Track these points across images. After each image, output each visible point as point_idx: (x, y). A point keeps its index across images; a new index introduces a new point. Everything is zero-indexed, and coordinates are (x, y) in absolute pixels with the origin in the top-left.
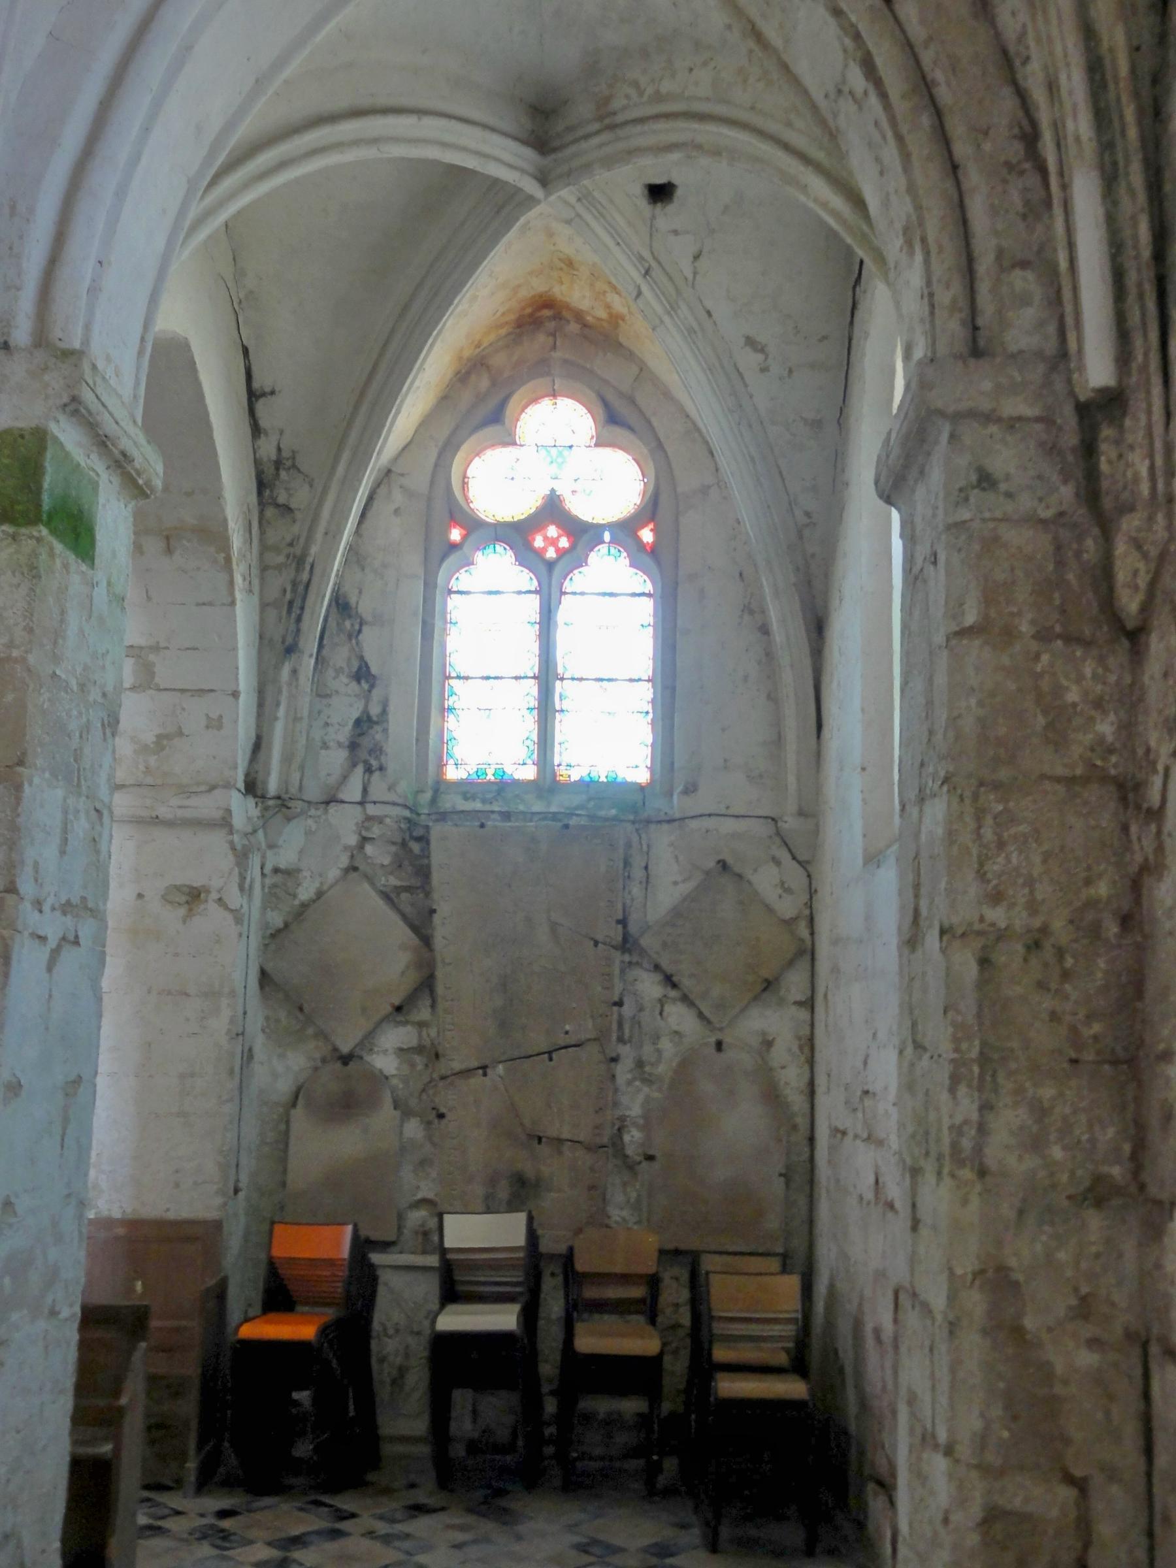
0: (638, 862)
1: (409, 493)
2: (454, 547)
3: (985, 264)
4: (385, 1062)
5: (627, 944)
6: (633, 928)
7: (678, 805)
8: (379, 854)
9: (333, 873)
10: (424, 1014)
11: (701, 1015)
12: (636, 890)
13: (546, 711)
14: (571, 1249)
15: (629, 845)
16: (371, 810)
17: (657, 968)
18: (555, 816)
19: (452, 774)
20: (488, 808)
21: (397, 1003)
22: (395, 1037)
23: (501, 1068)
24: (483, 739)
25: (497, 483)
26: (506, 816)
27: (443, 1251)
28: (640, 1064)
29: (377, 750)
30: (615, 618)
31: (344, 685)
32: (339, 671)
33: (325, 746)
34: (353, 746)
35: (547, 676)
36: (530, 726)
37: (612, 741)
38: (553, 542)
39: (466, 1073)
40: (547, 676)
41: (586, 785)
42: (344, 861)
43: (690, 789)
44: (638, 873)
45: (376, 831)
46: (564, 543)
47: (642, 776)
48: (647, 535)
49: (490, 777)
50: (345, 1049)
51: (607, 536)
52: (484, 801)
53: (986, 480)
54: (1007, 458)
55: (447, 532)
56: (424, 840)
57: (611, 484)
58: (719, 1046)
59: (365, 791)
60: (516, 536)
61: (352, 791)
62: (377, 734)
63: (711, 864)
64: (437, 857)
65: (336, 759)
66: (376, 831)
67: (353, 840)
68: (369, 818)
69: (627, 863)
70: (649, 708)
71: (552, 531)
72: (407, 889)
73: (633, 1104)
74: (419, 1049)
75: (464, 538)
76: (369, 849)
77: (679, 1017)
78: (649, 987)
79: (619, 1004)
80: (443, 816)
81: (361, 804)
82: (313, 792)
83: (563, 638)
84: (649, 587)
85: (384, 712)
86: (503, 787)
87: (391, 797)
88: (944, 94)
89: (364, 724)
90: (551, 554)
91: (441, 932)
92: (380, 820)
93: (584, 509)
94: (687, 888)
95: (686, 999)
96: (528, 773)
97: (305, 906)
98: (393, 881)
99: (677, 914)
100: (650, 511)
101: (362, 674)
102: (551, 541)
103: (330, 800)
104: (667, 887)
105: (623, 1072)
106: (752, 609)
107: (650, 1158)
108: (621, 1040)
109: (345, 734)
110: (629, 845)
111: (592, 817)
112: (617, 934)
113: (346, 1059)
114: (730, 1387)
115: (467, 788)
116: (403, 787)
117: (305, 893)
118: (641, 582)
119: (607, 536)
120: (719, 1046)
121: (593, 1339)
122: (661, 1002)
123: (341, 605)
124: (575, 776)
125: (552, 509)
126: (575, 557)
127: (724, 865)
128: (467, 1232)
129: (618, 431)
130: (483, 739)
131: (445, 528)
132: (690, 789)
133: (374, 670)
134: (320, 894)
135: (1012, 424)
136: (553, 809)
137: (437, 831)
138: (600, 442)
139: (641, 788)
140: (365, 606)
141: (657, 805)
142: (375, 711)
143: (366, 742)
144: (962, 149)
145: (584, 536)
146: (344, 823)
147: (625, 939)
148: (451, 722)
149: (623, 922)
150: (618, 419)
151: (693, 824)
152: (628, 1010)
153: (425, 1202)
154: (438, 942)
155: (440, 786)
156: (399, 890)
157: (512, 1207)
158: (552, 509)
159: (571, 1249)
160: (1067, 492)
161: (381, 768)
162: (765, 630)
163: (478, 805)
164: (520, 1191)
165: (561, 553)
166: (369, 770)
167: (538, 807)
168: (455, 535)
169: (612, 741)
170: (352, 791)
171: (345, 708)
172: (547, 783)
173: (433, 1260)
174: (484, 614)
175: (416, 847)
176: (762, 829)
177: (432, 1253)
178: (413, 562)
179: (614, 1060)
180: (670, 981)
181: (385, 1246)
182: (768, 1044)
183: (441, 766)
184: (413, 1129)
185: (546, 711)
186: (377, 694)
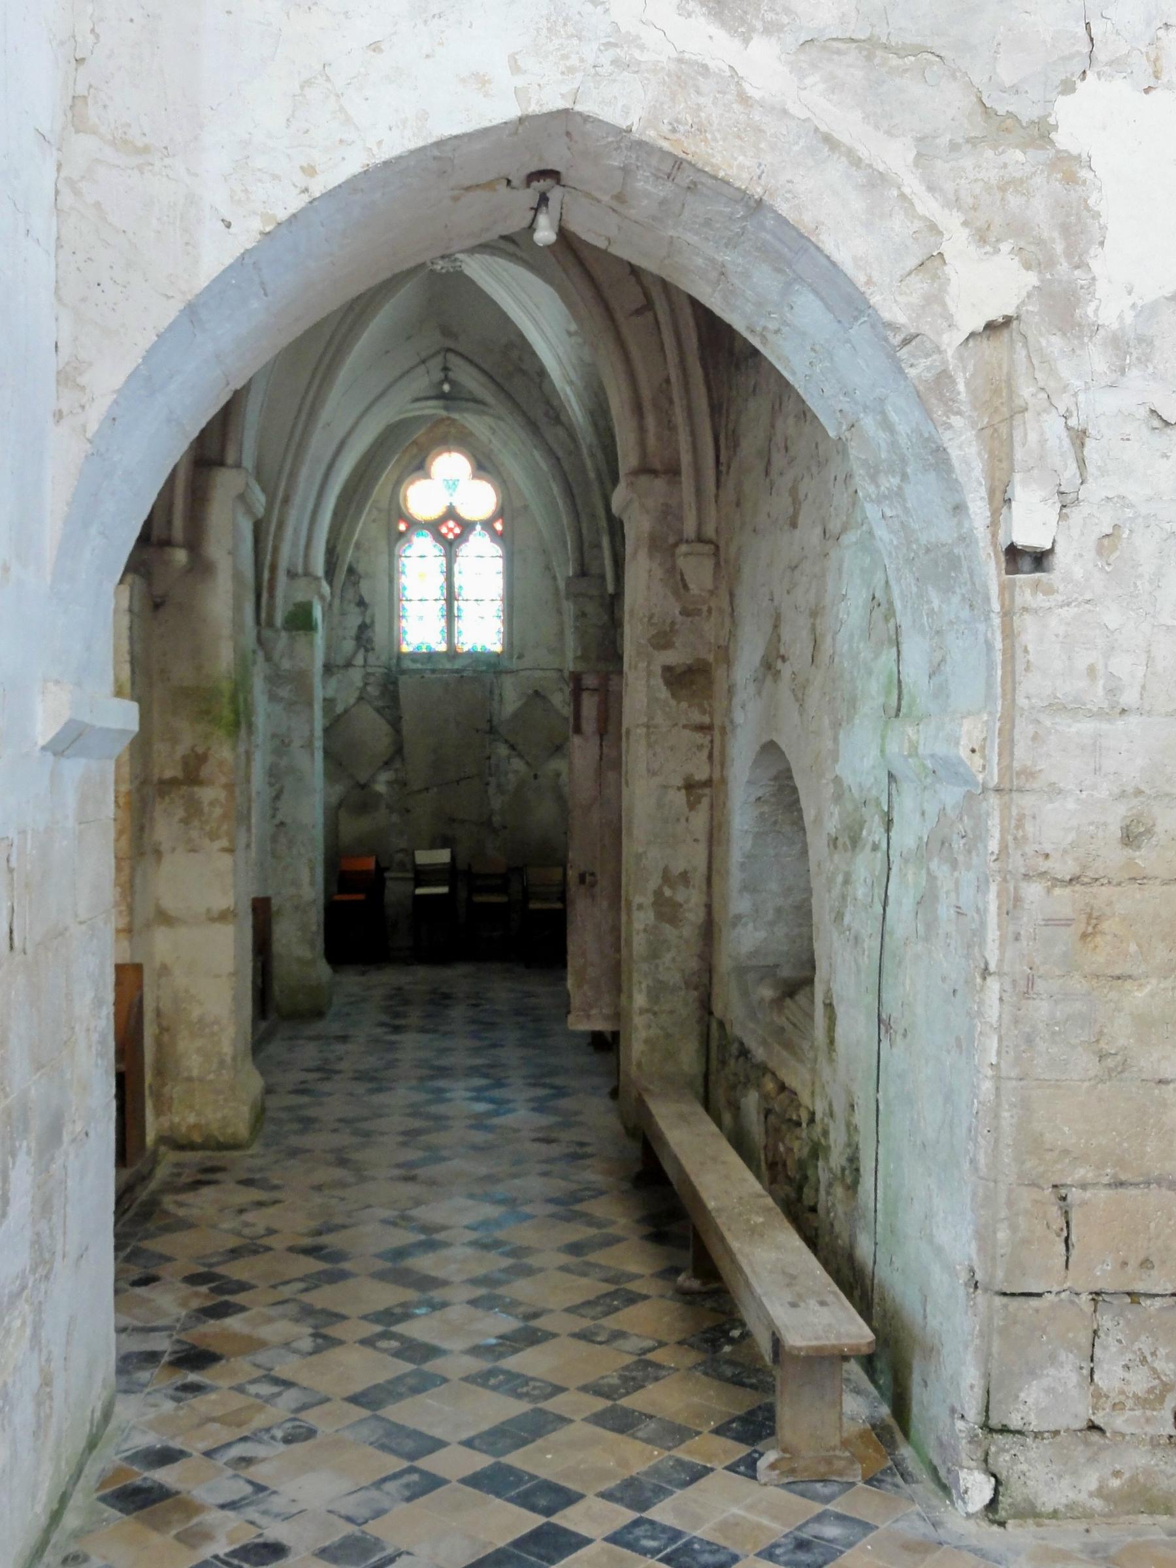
0: (497, 692)
1: (379, 510)
2: (401, 535)
3: (586, 545)
4: (380, 787)
5: (492, 730)
6: (494, 723)
7: (515, 664)
8: (373, 691)
9: (352, 701)
10: (397, 765)
11: (527, 763)
12: (496, 705)
13: (450, 616)
14: (469, 865)
15: (492, 683)
16: (370, 670)
17: (506, 741)
18: (457, 671)
19: (405, 648)
20: (424, 667)
21: (385, 759)
22: (384, 777)
23: (435, 790)
24: (419, 631)
25: (423, 498)
26: (433, 671)
27: (415, 865)
28: (499, 786)
29: (370, 640)
30: (483, 568)
31: (353, 609)
32: (350, 602)
33: (345, 638)
34: (358, 638)
35: (450, 597)
36: (443, 623)
37: (483, 631)
38: (451, 530)
39: (420, 792)
40: (450, 597)
41: (469, 654)
42: (356, 694)
43: (520, 657)
44: (496, 697)
45: (372, 679)
46: (457, 531)
47: (498, 648)
48: (498, 526)
49: (424, 650)
50: (362, 782)
51: (478, 527)
52: (422, 664)
53: (584, 615)
54: (590, 608)
55: (397, 525)
56: (395, 683)
57: (480, 500)
58: (536, 777)
59: (365, 661)
60: (433, 527)
61: (359, 660)
62: (369, 633)
63: (530, 692)
64: (403, 693)
65: (349, 645)
66: (372, 679)
67: (360, 684)
68: (368, 674)
69: (491, 692)
70: (501, 614)
71: (451, 524)
72: (388, 707)
73: (497, 803)
74: (396, 781)
75: (408, 528)
76: (369, 688)
77: (517, 764)
78: (503, 750)
79: (489, 758)
80: (403, 672)
81: (364, 667)
82: (340, 661)
83: (458, 581)
84: (500, 553)
85: (373, 622)
86: (431, 656)
87: (377, 663)
88: (575, 491)
89: (363, 627)
90: (451, 536)
91: (406, 728)
92: (373, 674)
93: (466, 513)
94: (518, 704)
95: (521, 756)
96: (442, 648)
97: (339, 716)
98: (380, 704)
99: (516, 715)
100: (500, 513)
101: (361, 603)
102: (450, 532)
103: (349, 665)
104: (510, 700)
105: (491, 790)
106: (548, 568)
107: (505, 827)
108: (491, 775)
109: (353, 632)
110: (492, 683)
111: (474, 671)
112: (486, 727)
113: (363, 787)
114: (534, 905)
115: (414, 656)
116: (384, 658)
117: (339, 709)
118: (496, 550)
119: (478, 527)
120: (536, 777)
121: (479, 899)
122: (509, 758)
123: (351, 571)
124: (465, 649)
125: (451, 514)
126: (461, 538)
127: (536, 693)
128: (424, 857)
129: (482, 473)
130: (419, 631)
131: (397, 527)
132: (520, 657)
133: (367, 600)
134: (346, 711)
135: (591, 598)
136: (456, 667)
137: (403, 679)
138: (475, 476)
139: (498, 655)
140: (361, 568)
141: (506, 663)
142: (368, 621)
143: (364, 637)
144: (580, 508)
145: (467, 527)
146: (356, 676)
147: (491, 728)
148: (404, 623)
149: (490, 721)
150: (483, 466)
151: (522, 673)
152: (493, 761)
153: (402, 850)
154: (405, 732)
155: (400, 656)
156: (383, 708)
157: (443, 847)
158: (451, 514)
159: (469, 865)
160: (606, 618)
161: (373, 649)
162: (554, 578)
163: (419, 666)
164: (444, 842)
165: (457, 536)
166: (367, 650)
167: (448, 666)
168: (402, 527)
169: (483, 631)
170: (359, 660)
171: (353, 621)
172: (452, 654)
173: (410, 875)
174: (418, 567)
175: (391, 687)
176: (553, 675)
177: (407, 871)
178: (382, 544)
179: (487, 784)
180: (513, 747)
181: (387, 869)
182: (558, 775)
183: (399, 645)
184: (395, 818)
185: (450, 616)
186: (368, 613)
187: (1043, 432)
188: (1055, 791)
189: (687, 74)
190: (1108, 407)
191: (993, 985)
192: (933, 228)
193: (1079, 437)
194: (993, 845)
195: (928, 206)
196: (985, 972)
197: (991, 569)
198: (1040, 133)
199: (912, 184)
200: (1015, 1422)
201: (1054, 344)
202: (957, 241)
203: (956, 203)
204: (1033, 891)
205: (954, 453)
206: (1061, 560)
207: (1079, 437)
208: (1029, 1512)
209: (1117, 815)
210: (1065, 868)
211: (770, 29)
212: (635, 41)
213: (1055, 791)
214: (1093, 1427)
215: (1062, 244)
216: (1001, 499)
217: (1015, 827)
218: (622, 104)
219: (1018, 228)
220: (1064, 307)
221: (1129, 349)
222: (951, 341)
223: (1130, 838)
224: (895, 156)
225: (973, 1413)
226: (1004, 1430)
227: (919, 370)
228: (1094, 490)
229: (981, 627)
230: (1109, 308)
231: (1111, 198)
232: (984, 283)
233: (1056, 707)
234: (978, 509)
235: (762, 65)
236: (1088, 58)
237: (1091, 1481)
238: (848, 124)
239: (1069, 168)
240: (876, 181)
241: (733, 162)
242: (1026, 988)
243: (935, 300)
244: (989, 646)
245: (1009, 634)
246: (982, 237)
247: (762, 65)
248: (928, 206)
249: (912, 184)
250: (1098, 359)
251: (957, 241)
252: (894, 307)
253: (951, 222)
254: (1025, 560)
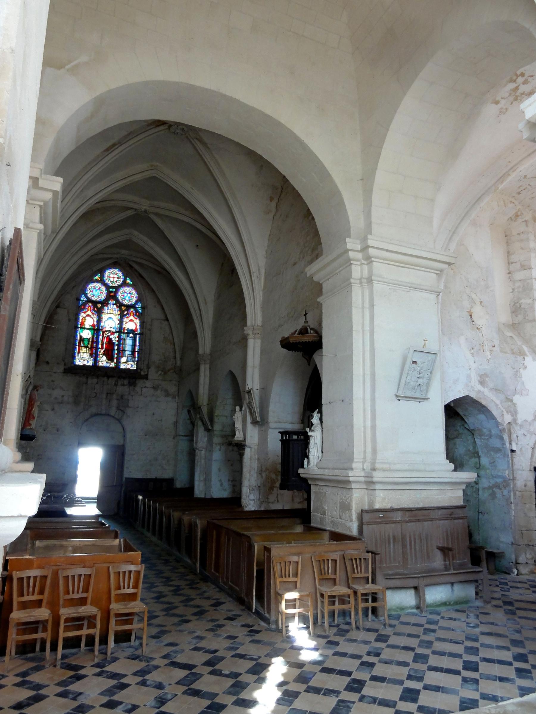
187: (514, 436)
188: (518, 480)
189: (479, 392)
190: (520, 433)
191: (513, 505)
192: (503, 411)
193: (517, 436)
194: (512, 487)
195: (502, 409)
196: (511, 503)
197: (509, 452)
198: (512, 401)
199: (500, 406)
200: (519, 562)
201: (514, 425)
202: (505, 413)
203: (504, 408)
204: (517, 492)
205: (505, 438)
206: (517, 451)
207: (517, 436)
208: (521, 574)
209: (524, 483)
210: (520, 490)
211: (487, 387)
212: (473, 387)
213: (518, 480)
214: (527, 563)
215: (514, 413)
216: (511, 444)
217: (515, 485)
218: (473, 395)
219: (510, 412)
220: (515, 420)
221: (521, 426)
222: (505, 424)
223: (525, 486)
224: (498, 402)
225: (514, 562)
226: (518, 563)
227: (501, 427)
228: (519, 443)
229: (506, 459)
230: (519, 421)
231: (519, 409)
232: (508, 418)
233: (518, 470)
234: (507, 444)
235: (486, 391)
236: (516, 392)
237: (527, 570)
238: (494, 399)
239: (515, 405)
240: (497, 405)
241: (484, 402)
242: (516, 505)
243: (503, 420)
244: (508, 462)
245: (512, 460)
246: (507, 412)
247: (486, 391)
248: (502, 409)
249: (500, 406)
250: (519, 428)
251: (505, 413)
252: (499, 420)
253: (504, 410)
254: (513, 451)
